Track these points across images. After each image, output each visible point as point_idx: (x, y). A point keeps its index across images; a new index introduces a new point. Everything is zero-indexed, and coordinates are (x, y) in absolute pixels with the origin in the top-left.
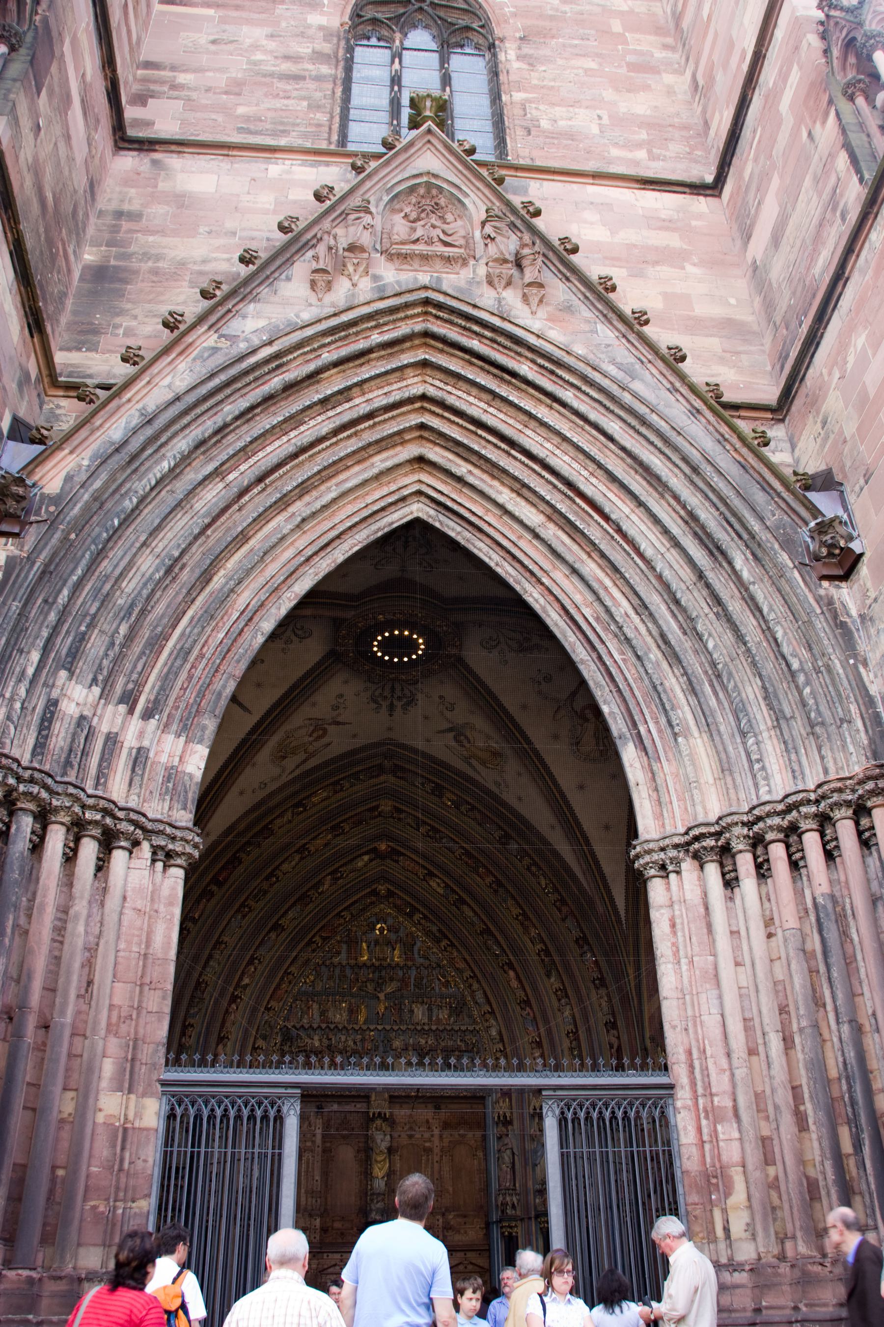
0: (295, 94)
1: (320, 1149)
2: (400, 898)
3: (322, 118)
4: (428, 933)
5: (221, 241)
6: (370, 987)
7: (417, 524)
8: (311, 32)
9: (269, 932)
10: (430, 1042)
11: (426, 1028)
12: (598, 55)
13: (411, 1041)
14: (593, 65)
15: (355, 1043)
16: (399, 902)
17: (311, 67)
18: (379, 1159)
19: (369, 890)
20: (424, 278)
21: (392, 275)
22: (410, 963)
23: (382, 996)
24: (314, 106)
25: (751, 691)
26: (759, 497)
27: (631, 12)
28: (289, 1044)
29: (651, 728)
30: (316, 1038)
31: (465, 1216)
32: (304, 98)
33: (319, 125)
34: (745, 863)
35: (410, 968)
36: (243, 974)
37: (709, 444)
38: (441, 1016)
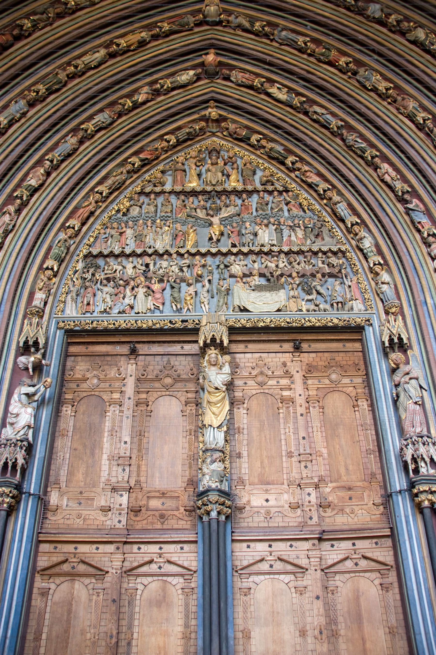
1: (131, 403)
2: (234, 121)
4: (271, 157)
6: (201, 214)
9: (66, 135)
10: (281, 265)
11: (275, 249)
13: (256, 265)
15: (181, 270)
16: (232, 127)
18: (213, 399)
19: (196, 116)
22: (250, 188)
23: (215, 220)
28: (91, 270)
30: (129, 266)
31: (350, 489)
35: (250, 193)
36: (26, 175)
38: (293, 238)
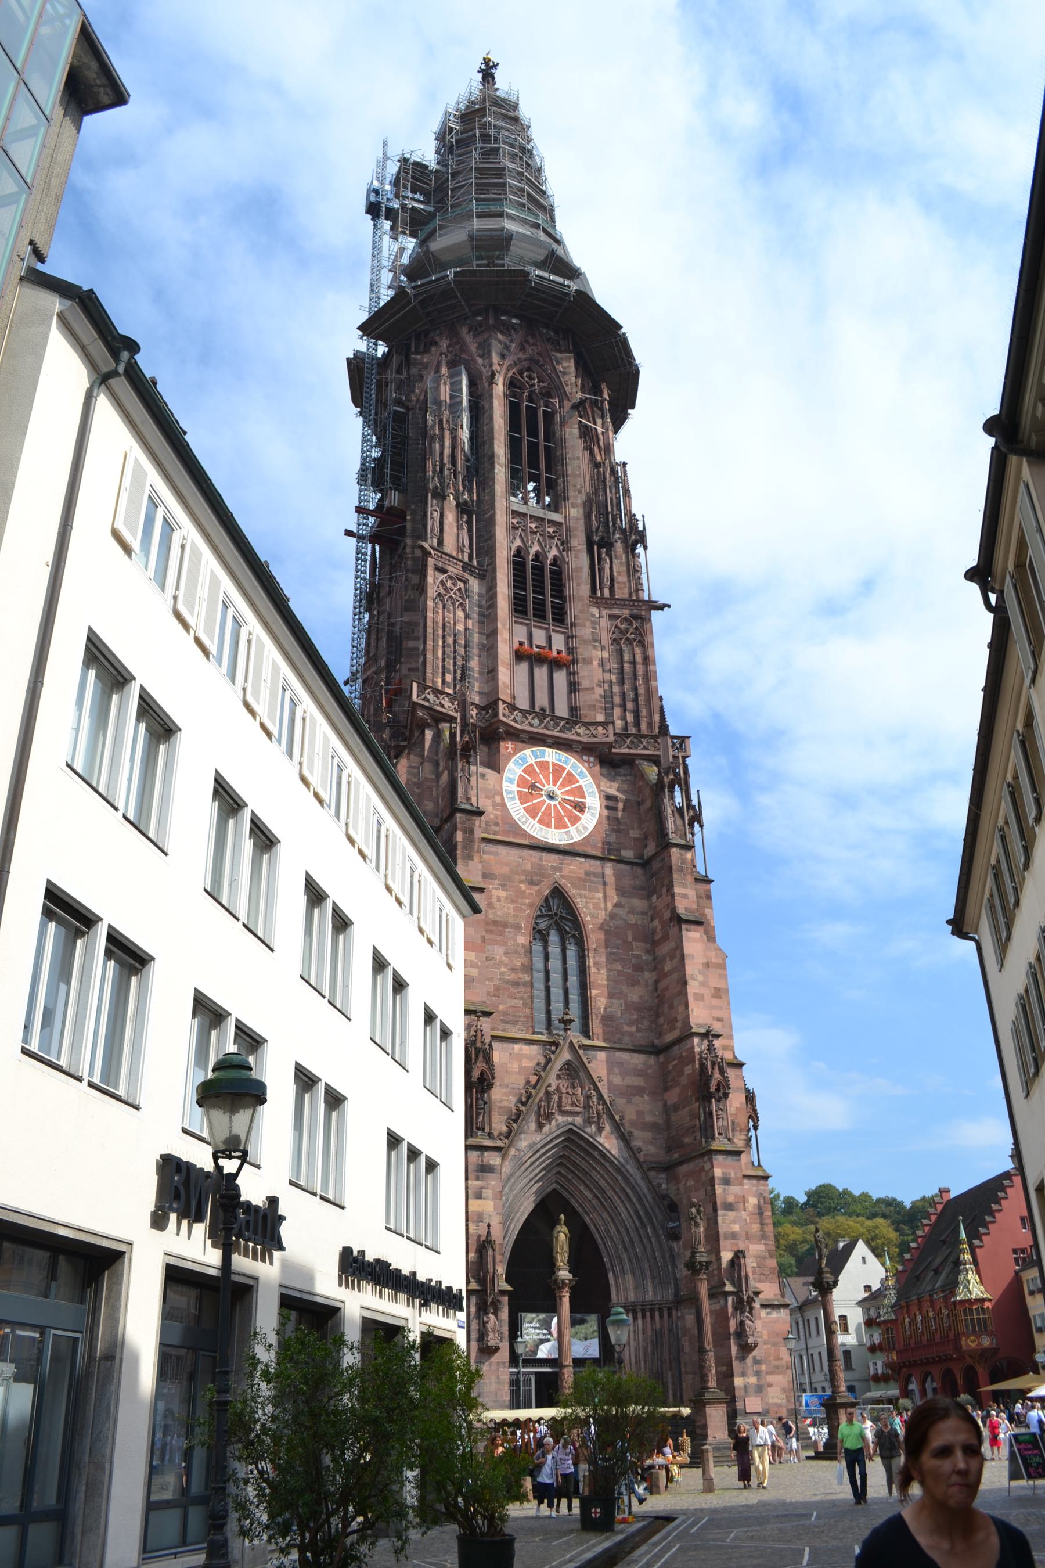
0: (518, 995)
3: (528, 1011)
5: (504, 1090)
7: (554, 1189)
8: (520, 949)
12: (622, 960)
14: (620, 968)
17: (521, 976)
20: (570, 1119)
21: (561, 1119)
24: (525, 1005)
25: (646, 1266)
26: (657, 1210)
27: (636, 924)
29: (617, 1268)
32: (521, 998)
33: (527, 1017)
34: (639, 1315)
37: (646, 1191)
